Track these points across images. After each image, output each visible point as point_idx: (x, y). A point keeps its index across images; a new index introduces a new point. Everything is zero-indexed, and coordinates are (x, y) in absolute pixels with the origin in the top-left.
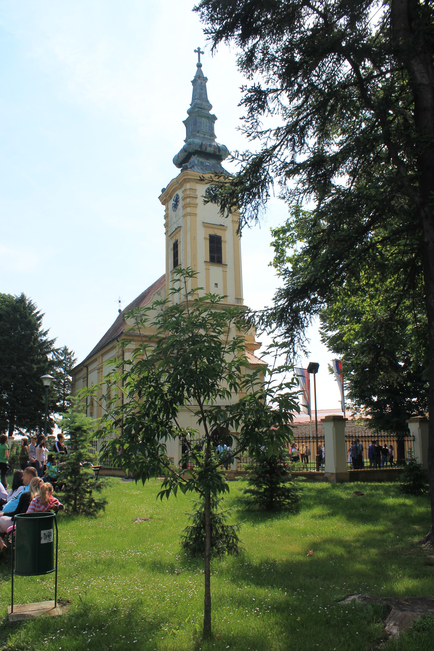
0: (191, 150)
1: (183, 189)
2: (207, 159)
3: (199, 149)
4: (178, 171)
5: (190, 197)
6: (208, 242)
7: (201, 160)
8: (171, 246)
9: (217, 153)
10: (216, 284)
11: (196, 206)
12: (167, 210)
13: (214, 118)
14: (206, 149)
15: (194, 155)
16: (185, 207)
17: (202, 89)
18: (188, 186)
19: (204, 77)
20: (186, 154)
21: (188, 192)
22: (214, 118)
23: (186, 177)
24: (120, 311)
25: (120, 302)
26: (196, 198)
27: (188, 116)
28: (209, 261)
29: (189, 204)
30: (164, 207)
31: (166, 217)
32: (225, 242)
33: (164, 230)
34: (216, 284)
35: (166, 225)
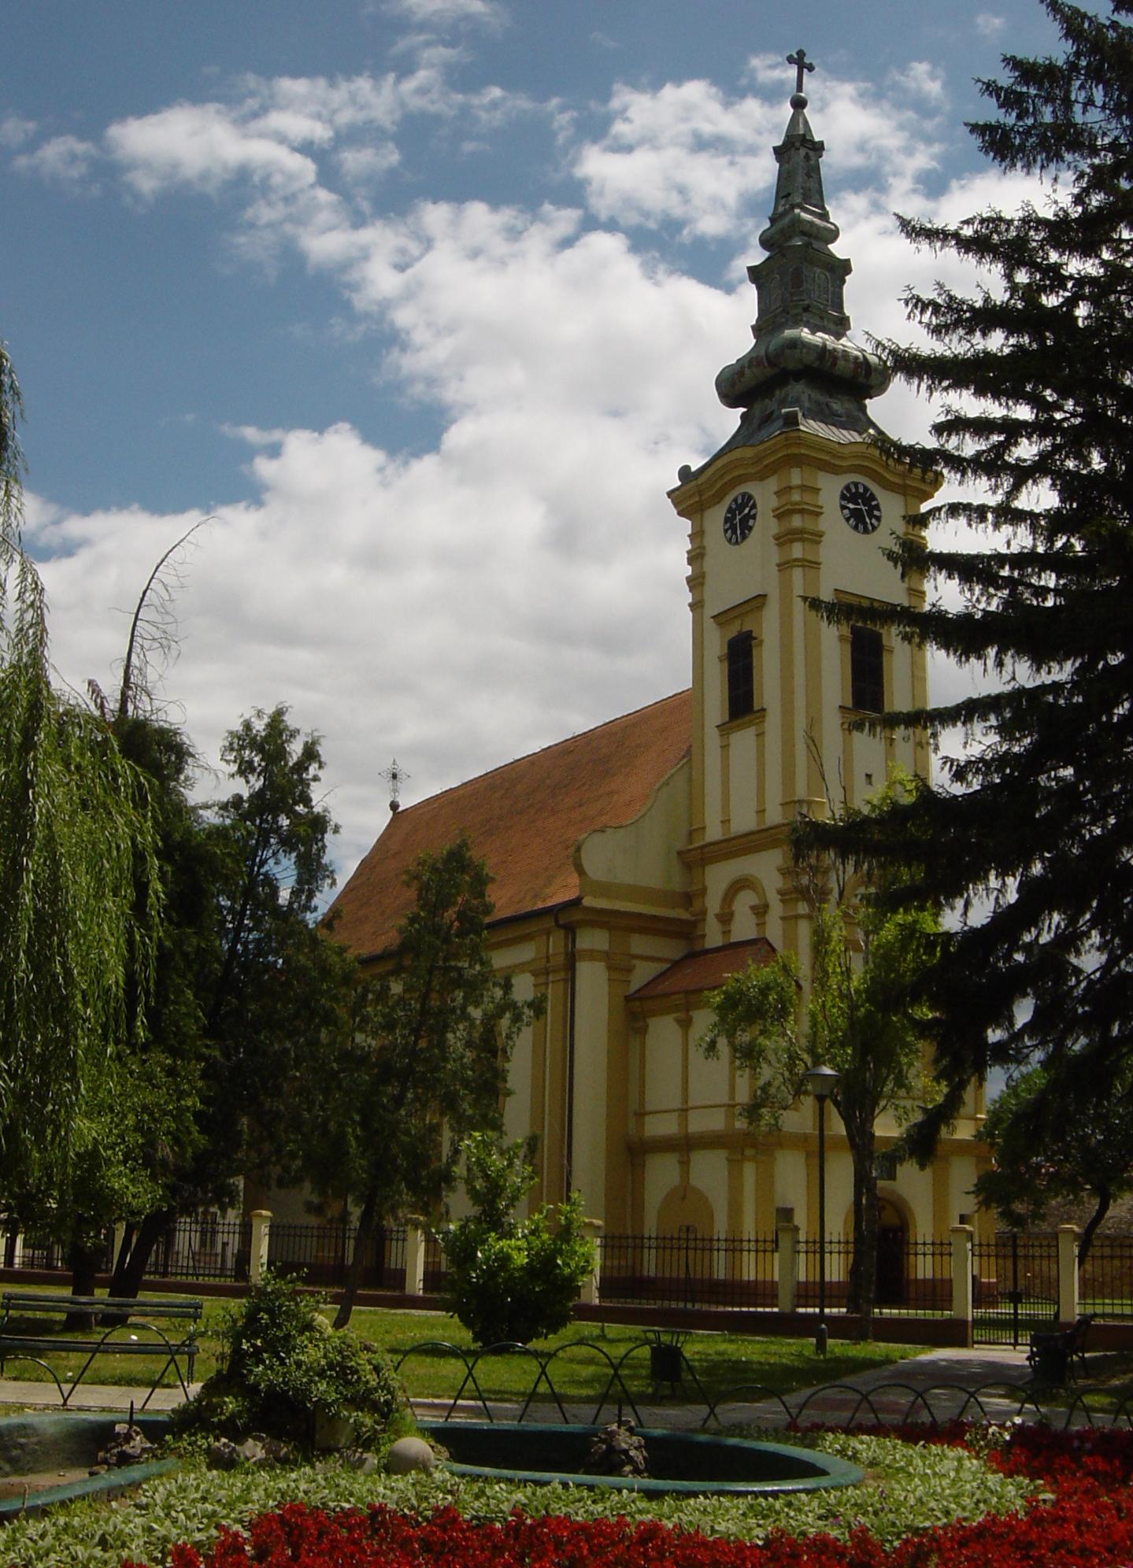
0: (791, 366)
1: (772, 484)
2: (831, 396)
3: (816, 364)
4: (731, 419)
5: (802, 512)
6: (848, 648)
7: (816, 395)
8: (716, 646)
9: (862, 379)
10: (869, 776)
11: (816, 538)
12: (697, 536)
13: (845, 267)
14: (834, 364)
15: (797, 380)
16: (784, 539)
17: (809, 175)
18: (796, 477)
19: (812, 142)
20: (770, 372)
21: (796, 497)
22: (845, 267)
23: (795, 451)
24: (394, 806)
25: (394, 776)
26: (818, 514)
27: (767, 254)
28: (850, 706)
29: (802, 531)
30: (686, 525)
31: (695, 557)
32: (891, 651)
33: (689, 598)
34: (869, 776)
35: (696, 582)
